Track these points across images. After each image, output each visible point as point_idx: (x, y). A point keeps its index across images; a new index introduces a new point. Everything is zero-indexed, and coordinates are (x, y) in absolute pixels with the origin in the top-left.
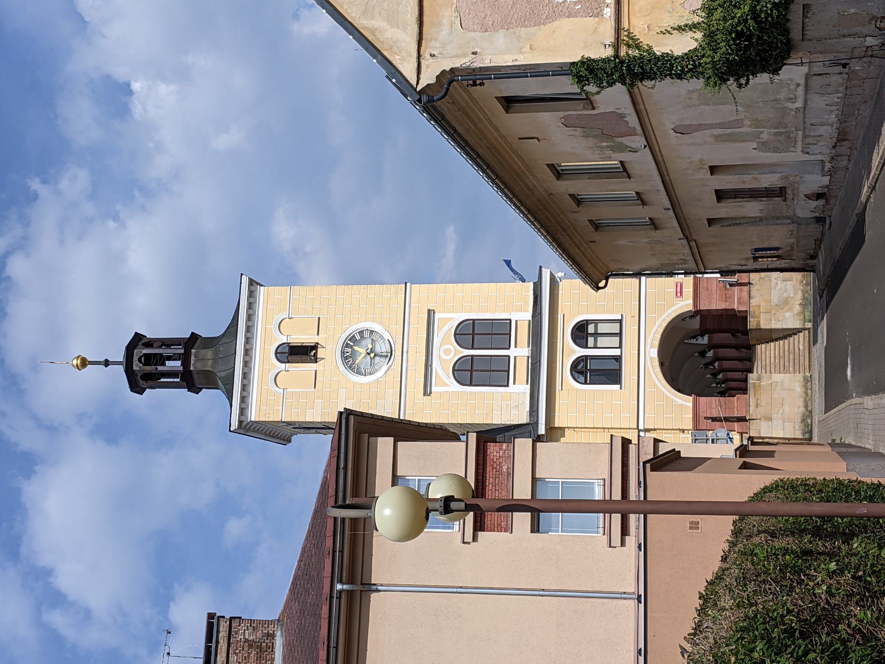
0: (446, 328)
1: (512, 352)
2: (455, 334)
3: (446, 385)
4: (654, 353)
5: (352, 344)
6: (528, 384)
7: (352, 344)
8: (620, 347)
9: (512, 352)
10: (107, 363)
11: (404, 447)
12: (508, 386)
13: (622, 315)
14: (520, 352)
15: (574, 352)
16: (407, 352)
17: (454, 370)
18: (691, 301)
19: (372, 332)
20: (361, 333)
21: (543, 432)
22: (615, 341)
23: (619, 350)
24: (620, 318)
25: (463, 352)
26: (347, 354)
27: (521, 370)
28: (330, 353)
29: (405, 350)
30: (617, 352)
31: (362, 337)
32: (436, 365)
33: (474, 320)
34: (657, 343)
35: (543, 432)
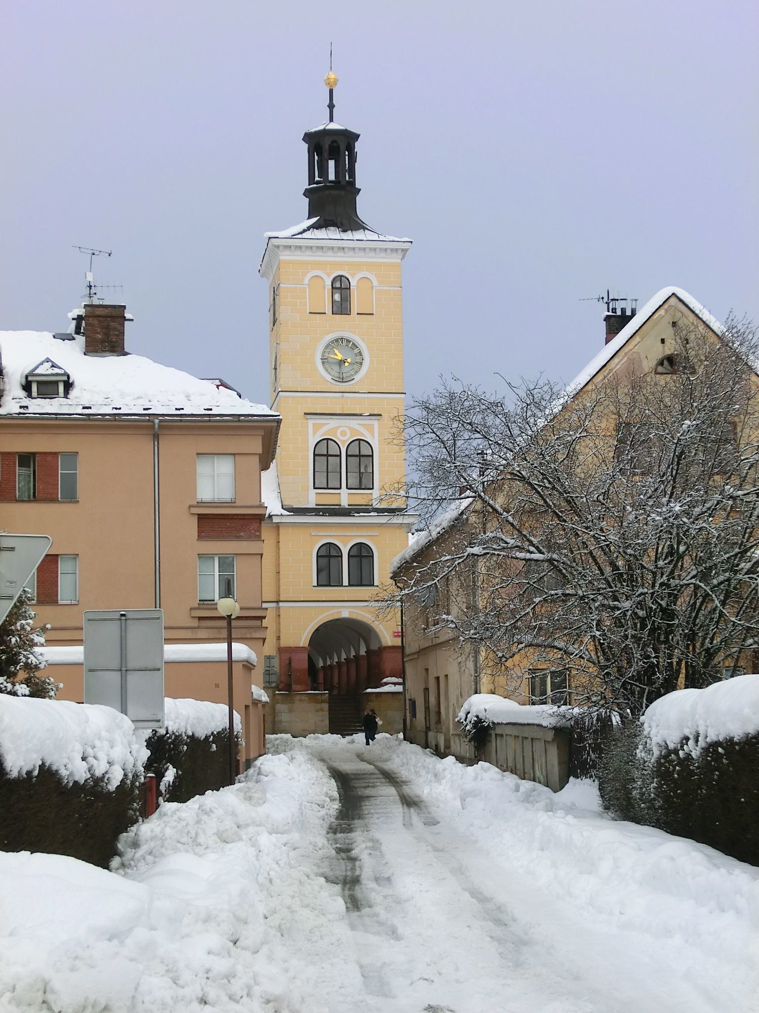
0: (362, 430)
1: (344, 491)
3: (314, 434)
4: (345, 614)
5: (350, 346)
7: (350, 346)
8: (350, 585)
9: (344, 491)
13: (377, 586)
14: (345, 498)
15: (345, 546)
18: (390, 644)
19: (361, 364)
20: (360, 354)
21: (274, 521)
23: (347, 585)
24: (375, 585)
25: (343, 447)
26: (341, 342)
27: (329, 498)
28: (342, 326)
29: (345, 394)
30: (346, 582)
32: (333, 423)
34: (354, 617)
35: (274, 521)
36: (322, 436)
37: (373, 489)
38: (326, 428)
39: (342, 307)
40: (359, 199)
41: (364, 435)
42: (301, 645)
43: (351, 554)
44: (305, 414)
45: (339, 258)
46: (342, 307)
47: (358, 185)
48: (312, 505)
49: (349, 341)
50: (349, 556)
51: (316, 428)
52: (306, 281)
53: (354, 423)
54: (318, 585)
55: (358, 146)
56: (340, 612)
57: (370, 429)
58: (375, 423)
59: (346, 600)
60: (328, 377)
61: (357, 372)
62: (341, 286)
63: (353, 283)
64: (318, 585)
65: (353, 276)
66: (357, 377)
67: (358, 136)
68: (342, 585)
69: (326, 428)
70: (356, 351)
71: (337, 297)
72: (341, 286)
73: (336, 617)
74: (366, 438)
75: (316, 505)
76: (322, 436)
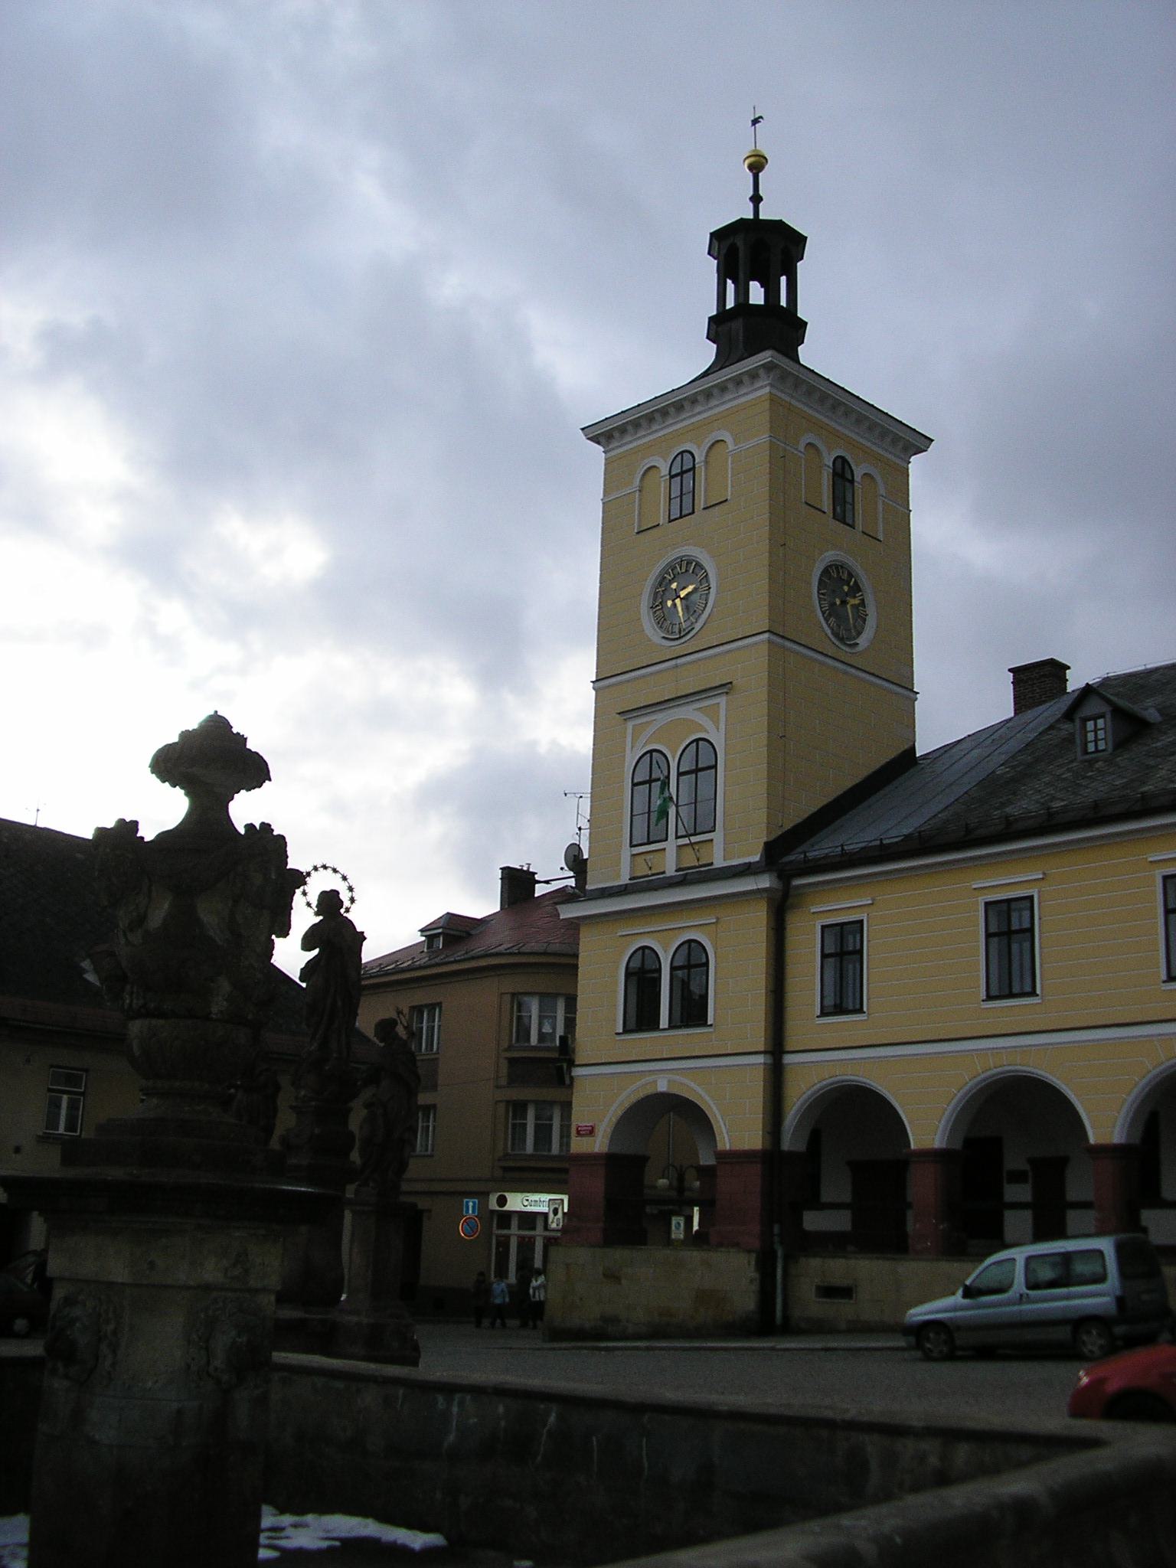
4: (662, 1086)
8: (671, 1027)
30: (664, 1022)
34: (675, 1091)
37: (714, 831)
38: (651, 730)
41: (706, 731)
48: (624, 879)
50: (673, 969)
56: (655, 1082)
57: (712, 713)
58: (722, 701)
59: (729, 1052)
64: (626, 1031)
69: (651, 730)
72: (684, 471)
73: (650, 1091)
74: (706, 731)
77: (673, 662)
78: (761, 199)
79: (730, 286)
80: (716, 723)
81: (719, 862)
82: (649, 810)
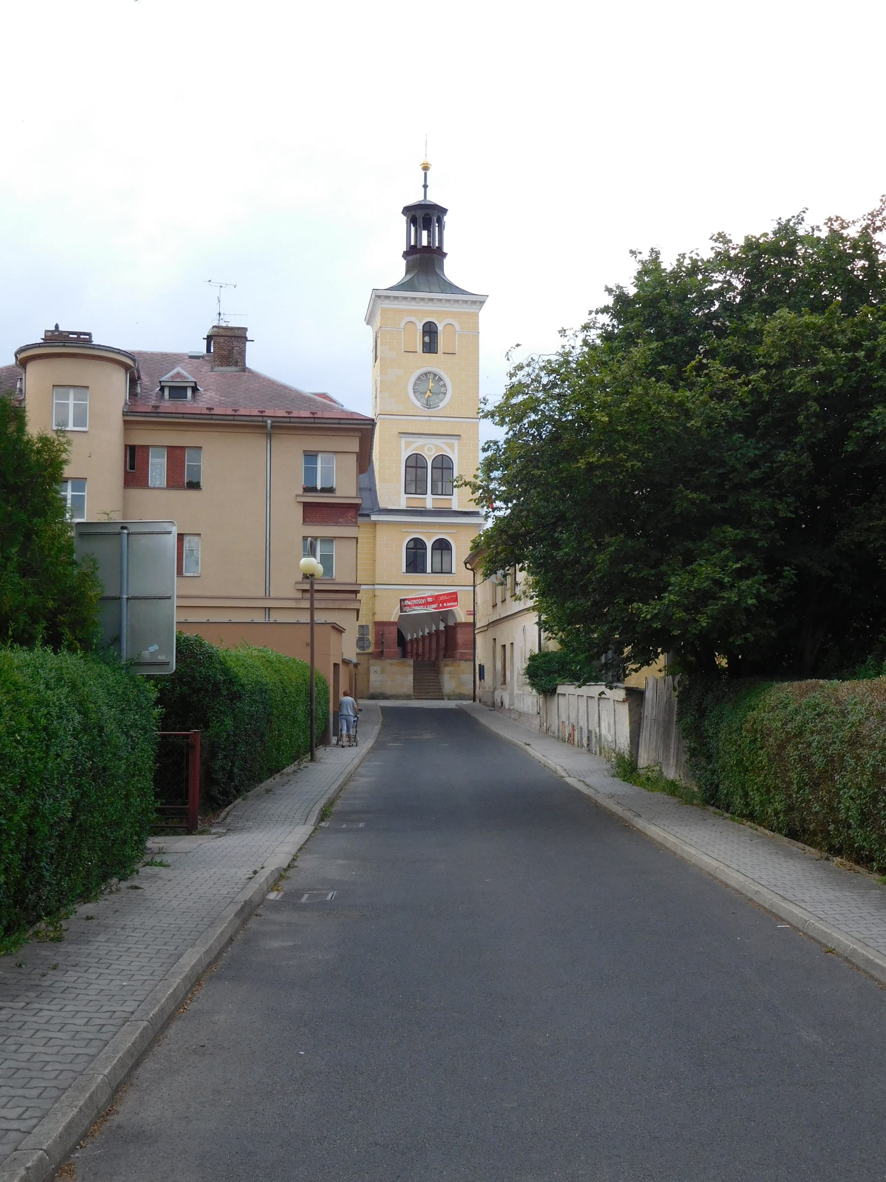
2: (442, 455)
6: (407, 507)
8: (432, 572)
10: (425, 186)
11: (354, 458)
12: (405, 493)
14: (429, 501)
16: (430, 420)
17: (417, 454)
18: (464, 621)
19: (445, 394)
20: (445, 385)
21: (372, 519)
22: (438, 567)
27: (416, 502)
28: (430, 362)
30: (429, 569)
31: (441, 386)
32: (421, 441)
33: (453, 468)
35: (372, 519)
36: (412, 451)
37: (452, 495)
39: (430, 347)
40: (446, 261)
41: (446, 452)
42: (392, 620)
43: (434, 547)
44: (399, 433)
45: (430, 307)
46: (430, 347)
47: (445, 250)
48: (403, 506)
49: (435, 375)
50: (432, 549)
51: (408, 445)
52: (402, 326)
53: (438, 442)
54: (407, 572)
55: (446, 219)
57: (452, 447)
58: (456, 442)
60: (419, 404)
61: (441, 401)
62: (430, 330)
63: (440, 328)
64: (407, 572)
65: (440, 322)
66: (442, 405)
67: (447, 210)
68: (426, 572)
70: (441, 383)
71: (427, 339)
72: (430, 330)
74: (446, 452)
75: (407, 507)
76: (412, 451)
77: (428, 418)
78: (427, 186)
79: (413, 229)
80: (453, 450)
81: (455, 507)
82: (416, 479)
